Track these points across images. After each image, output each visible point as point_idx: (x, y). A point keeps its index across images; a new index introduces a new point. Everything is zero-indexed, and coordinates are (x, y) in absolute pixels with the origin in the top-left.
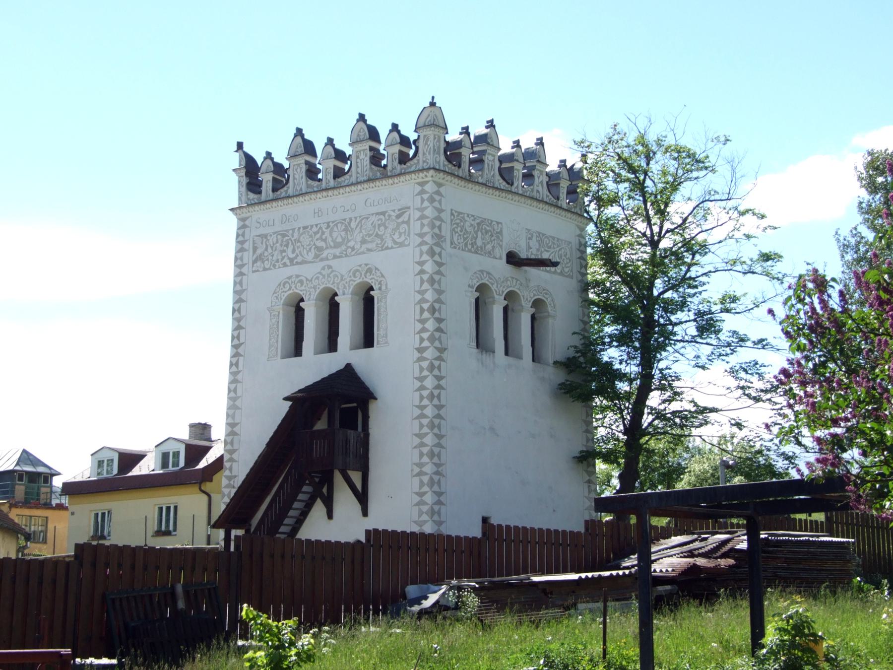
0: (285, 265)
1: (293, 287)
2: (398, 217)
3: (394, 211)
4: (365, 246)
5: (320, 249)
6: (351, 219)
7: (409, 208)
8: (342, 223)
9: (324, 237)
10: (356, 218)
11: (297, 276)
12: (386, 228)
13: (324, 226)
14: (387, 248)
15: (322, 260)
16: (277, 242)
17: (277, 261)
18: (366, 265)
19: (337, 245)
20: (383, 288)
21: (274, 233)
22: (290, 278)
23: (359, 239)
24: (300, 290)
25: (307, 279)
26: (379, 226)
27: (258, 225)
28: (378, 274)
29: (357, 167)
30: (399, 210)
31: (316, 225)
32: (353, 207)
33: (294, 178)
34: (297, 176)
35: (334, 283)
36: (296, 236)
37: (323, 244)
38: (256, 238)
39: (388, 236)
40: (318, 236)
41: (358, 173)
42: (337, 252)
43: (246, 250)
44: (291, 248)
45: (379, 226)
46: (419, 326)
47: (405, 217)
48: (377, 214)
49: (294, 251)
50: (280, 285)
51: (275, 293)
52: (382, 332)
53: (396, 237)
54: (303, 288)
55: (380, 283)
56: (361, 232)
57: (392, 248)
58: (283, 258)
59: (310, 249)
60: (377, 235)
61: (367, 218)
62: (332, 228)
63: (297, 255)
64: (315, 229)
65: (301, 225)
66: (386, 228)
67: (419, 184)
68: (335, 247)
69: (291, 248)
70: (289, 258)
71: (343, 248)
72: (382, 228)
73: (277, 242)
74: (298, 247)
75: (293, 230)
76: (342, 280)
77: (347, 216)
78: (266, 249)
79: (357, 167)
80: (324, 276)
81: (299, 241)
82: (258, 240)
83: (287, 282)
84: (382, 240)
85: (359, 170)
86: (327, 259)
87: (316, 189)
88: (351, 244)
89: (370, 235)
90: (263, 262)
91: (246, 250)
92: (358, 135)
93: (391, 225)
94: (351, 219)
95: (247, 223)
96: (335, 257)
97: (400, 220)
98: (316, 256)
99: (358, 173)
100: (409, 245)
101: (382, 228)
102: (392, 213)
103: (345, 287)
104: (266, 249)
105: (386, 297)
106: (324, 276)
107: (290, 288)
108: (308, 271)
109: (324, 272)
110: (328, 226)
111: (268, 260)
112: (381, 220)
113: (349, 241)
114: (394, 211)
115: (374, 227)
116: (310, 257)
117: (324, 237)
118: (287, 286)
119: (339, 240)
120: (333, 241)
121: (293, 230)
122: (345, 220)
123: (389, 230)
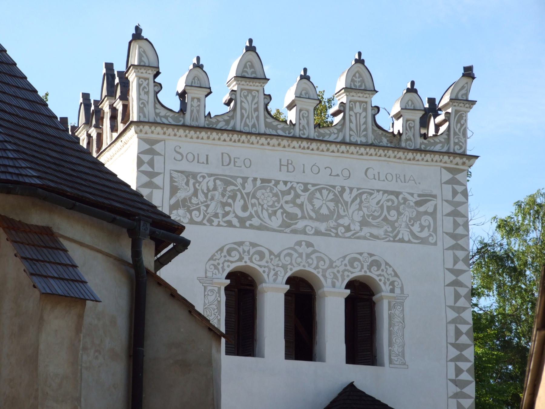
0: (230, 224)
1: (246, 258)
2: (419, 204)
3: (412, 195)
4: (366, 231)
5: (292, 217)
6: (343, 189)
7: (435, 196)
8: (330, 191)
9: (298, 201)
10: (351, 189)
11: (253, 245)
12: (400, 214)
13: (299, 188)
14: (402, 241)
15: (294, 232)
16: (215, 189)
17: (216, 215)
18: (371, 255)
19: (321, 218)
20: (397, 291)
21: (210, 175)
22: (241, 244)
23: (358, 217)
24: (254, 264)
25: (271, 253)
26: (389, 209)
27: (179, 157)
28: (390, 271)
29: (351, 121)
30: (419, 196)
31: (285, 183)
32: (346, 173)
33: (242, 108)
34: (246, 105)
35: (317, 267)
36: (249, 187)
37: (297, 211)
38: (175, 175)
39: (404, 225)
40: (289, 198)
41: (351, 129)
42: (322, 227)
43: (157, 187)
44: (239, 203)
45: (389, 209)
46: (454, 352)
47: (429, 207)
48: (385, 192)
49: (245, 208)
50: (221, 250)
51: (211, 259)
52: (396, 349)
53: (416, 228)
54: (263, 263)
55: (392, 283)
56: (360, 209)
57: (409, 242)
58: (226, 214)
59: (275, 213)
60: (385, 219)
61: (371, 194)
62: (313, 194)
63: (251, 217)
64: (281, 187)
65: (259, 176)
66: (400, 214)
67: (448, 169)
68: (317, 219)
69: (239, 203)
70: (237, 216)
71: (332, 223)
72: (393, 212)
73: (215, 189)
74: (253, 205)
75: (245, 179)
76: (331, 266)
77: (338, 182)
78: (195, 194)
79: (351, 121)
80: (300, 255)
81: (254, 197)
82: (181, 180)
83: (235, 249)
84: (394, 228)
86: (304, 232)
87: (280, 132)
88: (345, 221)
89: (375, 218)
90: (190, 212)
91: (157, 187)
92: (353, 80)
93: (408, 213)
94: (343, 189)
95: (158, 147)
96: (318, 233)
97: (422, 209)
98: (285, 225)
99: (351, 129)
100: (435, 244)
101: (393, 212)
102: (409, 197)
103: (335, 277)
104: (195, 194)
105: (402, 304)
106: (300, 255)
107: (241, 259)
108: (277, 242)
109: (300, 250)
110: (306, 190)
111: (199, 209)
112: (393, 202)
113: (340, 217)
114: (412, 195)
115: (382, 207)
116: (276, 222)
117: (298, 201)
118: (235, 255)
119: (324, 211)
120: (313, 210)
121: (245, 179)
122: (334, 187)
123: (404, 219)
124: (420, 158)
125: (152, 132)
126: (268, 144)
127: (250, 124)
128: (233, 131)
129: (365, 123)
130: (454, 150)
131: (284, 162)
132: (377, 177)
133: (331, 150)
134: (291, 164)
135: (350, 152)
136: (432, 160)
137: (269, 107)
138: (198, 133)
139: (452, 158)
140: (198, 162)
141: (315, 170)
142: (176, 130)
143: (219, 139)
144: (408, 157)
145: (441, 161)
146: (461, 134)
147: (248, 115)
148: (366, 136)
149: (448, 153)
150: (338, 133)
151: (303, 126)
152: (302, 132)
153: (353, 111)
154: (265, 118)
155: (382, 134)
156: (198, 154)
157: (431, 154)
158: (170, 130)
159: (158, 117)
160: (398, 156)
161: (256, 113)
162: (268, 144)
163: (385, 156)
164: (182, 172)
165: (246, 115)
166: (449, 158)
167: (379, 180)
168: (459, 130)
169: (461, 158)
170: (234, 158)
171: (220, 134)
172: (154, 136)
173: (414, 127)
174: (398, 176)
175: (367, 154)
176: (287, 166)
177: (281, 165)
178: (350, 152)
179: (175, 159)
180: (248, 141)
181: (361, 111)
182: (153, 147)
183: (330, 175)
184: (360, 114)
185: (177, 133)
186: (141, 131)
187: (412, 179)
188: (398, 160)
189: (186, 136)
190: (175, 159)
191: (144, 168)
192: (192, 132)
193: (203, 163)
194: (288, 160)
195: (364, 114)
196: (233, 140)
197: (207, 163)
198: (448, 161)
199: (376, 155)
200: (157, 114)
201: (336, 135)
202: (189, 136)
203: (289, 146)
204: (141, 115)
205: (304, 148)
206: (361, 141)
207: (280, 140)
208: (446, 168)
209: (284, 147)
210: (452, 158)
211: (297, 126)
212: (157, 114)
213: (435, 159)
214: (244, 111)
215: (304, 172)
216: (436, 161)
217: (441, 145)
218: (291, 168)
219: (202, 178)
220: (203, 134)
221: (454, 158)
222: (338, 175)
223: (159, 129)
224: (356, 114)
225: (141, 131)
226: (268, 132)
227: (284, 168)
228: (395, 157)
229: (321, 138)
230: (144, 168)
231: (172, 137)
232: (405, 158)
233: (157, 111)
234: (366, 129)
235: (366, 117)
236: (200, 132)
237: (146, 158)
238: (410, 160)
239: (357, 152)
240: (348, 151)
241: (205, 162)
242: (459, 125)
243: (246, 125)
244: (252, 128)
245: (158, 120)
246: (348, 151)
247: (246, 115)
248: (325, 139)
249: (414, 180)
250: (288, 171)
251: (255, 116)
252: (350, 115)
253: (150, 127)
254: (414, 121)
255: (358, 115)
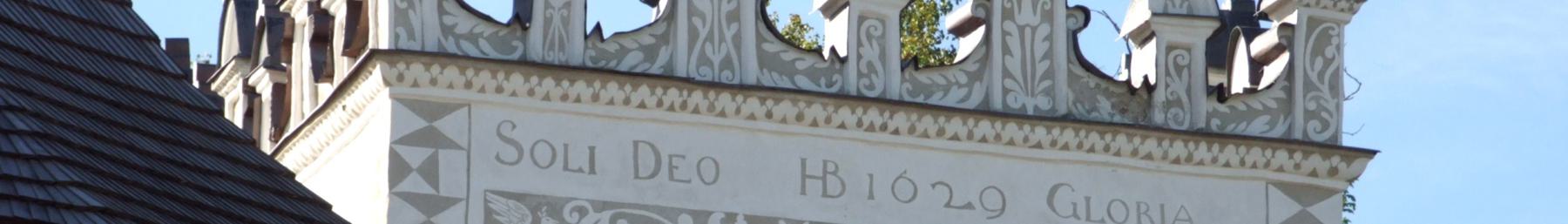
27: (510, 153)
29: (1006, 50)
32: (993, 200)
38: (499, 204)
41: (1006, 73)
67: (1289, 189)
79: (1006, 50)
85: (1014, 64)
87: (804, 83)
95: (449, 125)
99: (1006, 73)
124: (1208, 157)
125: (433, 82)
126: (769, 115)
127: (717, 60)
128: (668, 78)
129: (1049, 55)
130: (1305, 132)
131: (815, 168)
132: (1082, 211)
133: (949, 133)
134: (834, 173)
135: (1006, 138)
136: (1242, 163)
137: (769, 10)
138: (566, 83)
139: (1298, 156)
140: (566, 168)
141: (905, 189)
142: (501, 76)
143: (627, 102)
144: (1172, 155)
145: (1267, 165)
146: (1325, 88)
147: (711, 32)
148: (1049, 92)
149: (1287, 142)
150: (970, 85)
151: (870, 65)
152: (865, 81)
153: (1013, 20)
154: (760, 39)
155: (1097, 85)
156: (566, 146)
157: (1238, 146)
158: (485, 77)
159: (451, 39)
160: (1143, 150)
161: (734, 26)
162: (769, 115)
163: (1107, 149)
164: (519, 197)
165: (703, 33)
166: (1291, 157)
167: (1088, 219)
168: (1321, 75)
169: (1326, 157)
170: (671, 157)
171: (628, 88)
172: (438, 94)
173: (1189, 66)
174: (1143, 208)
175: (1054, 144)
176: (824, 179)
177: (804, 176)
178: (1006, 138)
179: (498, 158)
180: (711, 108)
181: (1035, 20)
182: (436, 124)
183: (948, 205)
184: (1034, 29)
185: (505, 84)
186: (401, 78)
187: (1183, 215)
188: (1143, 163)
189: (531, 93)
190: (498, 158)
191: (407, 185)
192: (549, 82)
193: (580, 170)
194: (825, 163)
195: (1044, 30)
196: (667, 103)
197: (592, 171)
198: (1289, 164)
199: (1080, 146)
200: (447, 30)
201: (964, 91)
202: (540, 91)
203: (828, 121)
204: (401, 31)
205: (871, 128)
206: (1036, 108)
207: (802, 105)
208: (1282, 186)
209: (815, 124)
210: (1298, 156)
211: (852, 63)
212: (447, 30)
213: (1249, 160)
214: (697, 21)
215: (871, 197)
216: (1254, 166)
217: (1266, 118)
218: (833, 185)
219: (576, 215)
220: (581, 87)
221: (1306, 155)
222: (969, 206)
223: (452, 72)
224: (1021, 29)
225: (401, 78)
226: (767, 82)
227: (814, 186)
228: (1135, 153)
229: (920, 99)
230: (407, 185)
231: (491, 96)
232: (1165, 157)
233: (448, 20)
234: (1049, 74)
235: (1049, 38)
236: (572, 82)
237: (415, 156)
238: (1177, 161)
239: (1026, 139)
240: (998, 137)
241: (586, 168)
242: (1319, 62)
243: (704, 60)
244: (721, 70)
245: (451, 47)
246: (998, 137)
247: (703, 33)
248: (934, 100)
249: (1190, 220)
250: (825, 194)
251: (729, 35)
252: (1005, 33)
253: (428, 67)
254: (1189, 50)
255: (1028, 31)
